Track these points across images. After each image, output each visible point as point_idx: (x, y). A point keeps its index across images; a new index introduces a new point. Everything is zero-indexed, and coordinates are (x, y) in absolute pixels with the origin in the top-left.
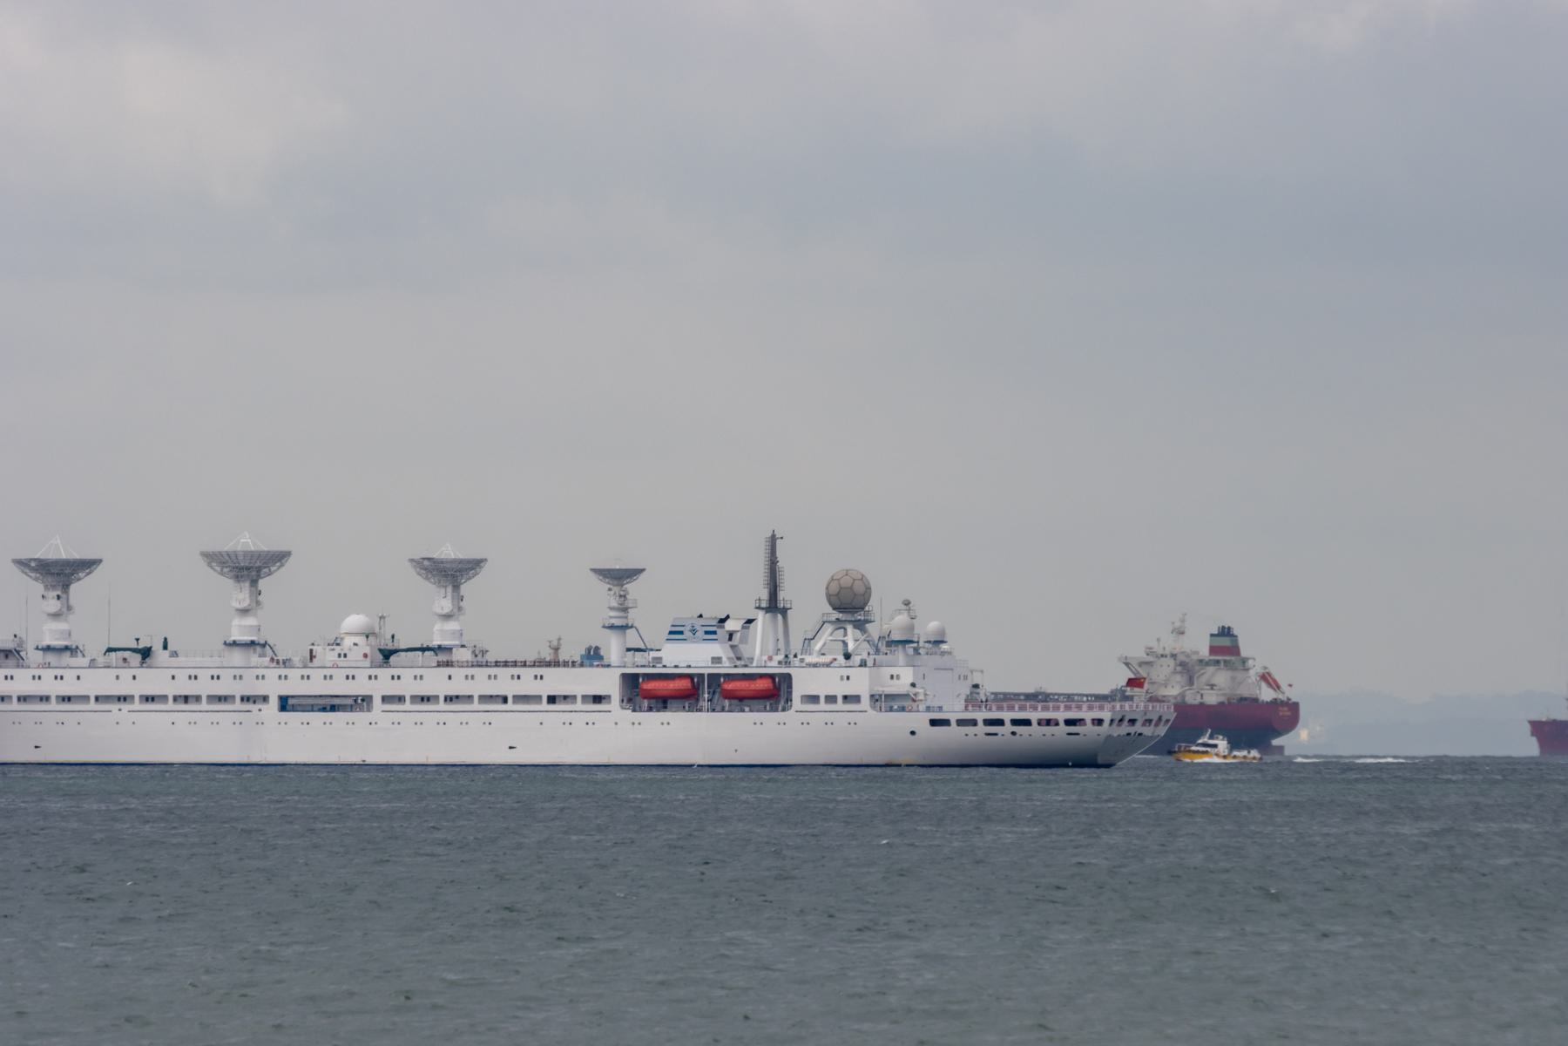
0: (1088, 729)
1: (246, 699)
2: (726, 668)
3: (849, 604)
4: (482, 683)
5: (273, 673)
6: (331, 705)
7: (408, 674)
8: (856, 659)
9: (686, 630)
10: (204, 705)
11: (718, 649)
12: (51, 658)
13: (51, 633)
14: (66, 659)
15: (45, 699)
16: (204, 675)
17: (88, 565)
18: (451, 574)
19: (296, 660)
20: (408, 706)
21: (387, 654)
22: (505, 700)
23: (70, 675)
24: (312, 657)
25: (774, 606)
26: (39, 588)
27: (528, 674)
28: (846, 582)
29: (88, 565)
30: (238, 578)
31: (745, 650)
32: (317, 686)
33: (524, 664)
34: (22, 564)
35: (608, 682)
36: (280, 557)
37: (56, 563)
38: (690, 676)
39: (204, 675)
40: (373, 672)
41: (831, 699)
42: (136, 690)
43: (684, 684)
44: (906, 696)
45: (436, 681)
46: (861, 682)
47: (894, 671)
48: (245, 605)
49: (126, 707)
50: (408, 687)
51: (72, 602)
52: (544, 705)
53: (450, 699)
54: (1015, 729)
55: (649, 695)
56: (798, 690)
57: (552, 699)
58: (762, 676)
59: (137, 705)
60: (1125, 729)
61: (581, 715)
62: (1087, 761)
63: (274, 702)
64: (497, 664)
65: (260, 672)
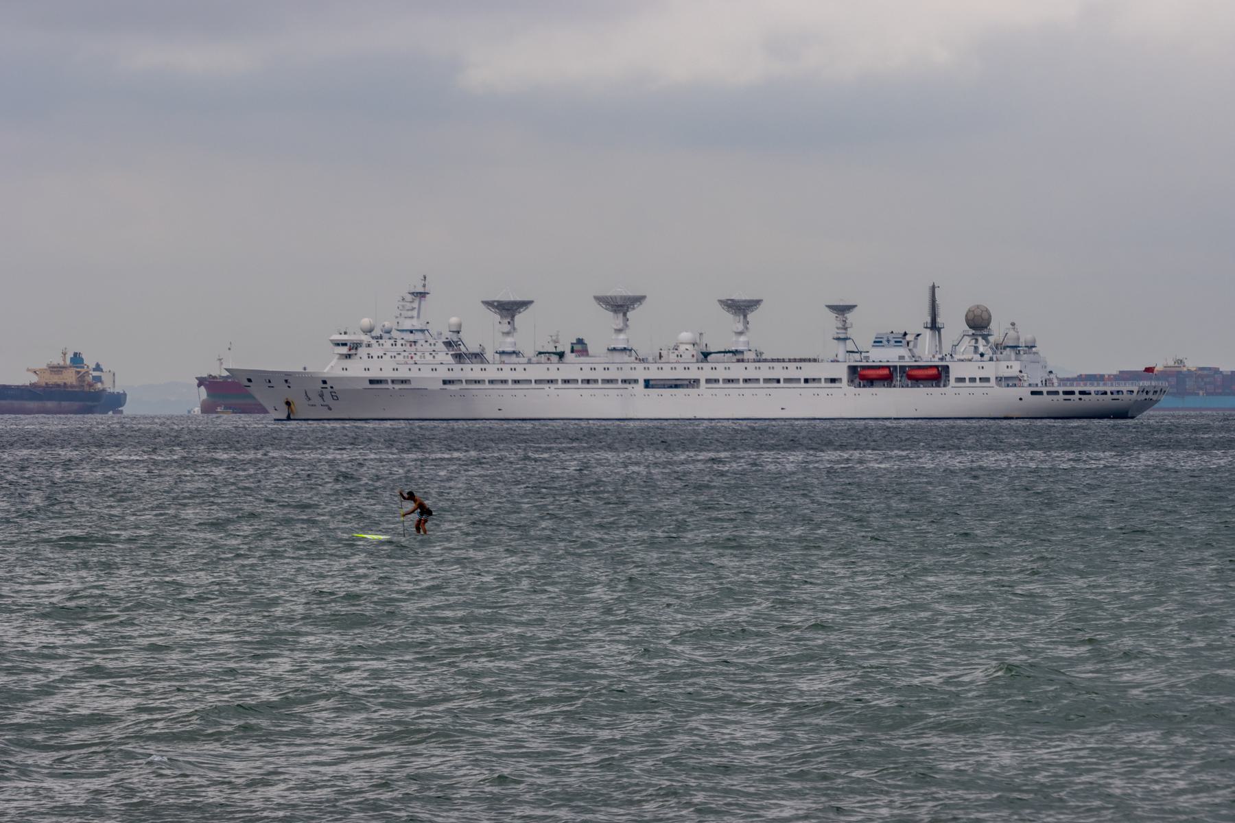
0: (1126, 396)
1: (624, 381)
2: (908, 362)
3: (978, 324)
4: (765, 371)
5: (640, 366)
6: (676, 385)
7: (720, 367)
8: (986, 357)
9: (884, 341)
10: (600, 385)
11: (902, 351)
12: (505, 358)
13: (507, 344)
14: (514, 358)
15: (504, 382)
16: (600, 368)
17: (525, 304)
18: (741, 308)
19: (650, 359)
20: (721, 384)
21: (706, 355)
22: (778, 381)
23: (520, 368)
24: (661, 357)
25: (934, 326)
26: (498, 317)
27: (792, 366)
28: (978, 312)
29: (525, 304)
30: (615, 311)
31: (917, 352)
32: (667, 374)
33: (790, 361)
34: (489, 304)
35: (842, 372)
36: (639, 299)
37: (509, 303)
38: (889, 367)
39: (600, 368)
40: (700, 365)
41: (973, 380)
42: (560, 376)
43: (886, 372)
44: (1016, 378)
45: (738, 371)
46: (990, 370)
47: (1009, 363)
48: (621, 326)
49: (553, 386)
50: (721, 374)
51: (516, 325)
52: (802, 384)
53: (746, 381)
54: (1083, 397)
55: (862, 378)
56: (953, 375)
57: (806, 381)
58: (931, 367)
59: (560, 385)
60: (1144, 396)
61: (824, 390)
62: (1122, 414)
63: (642, 383)
64: (773, 360)
65: (633, 365)
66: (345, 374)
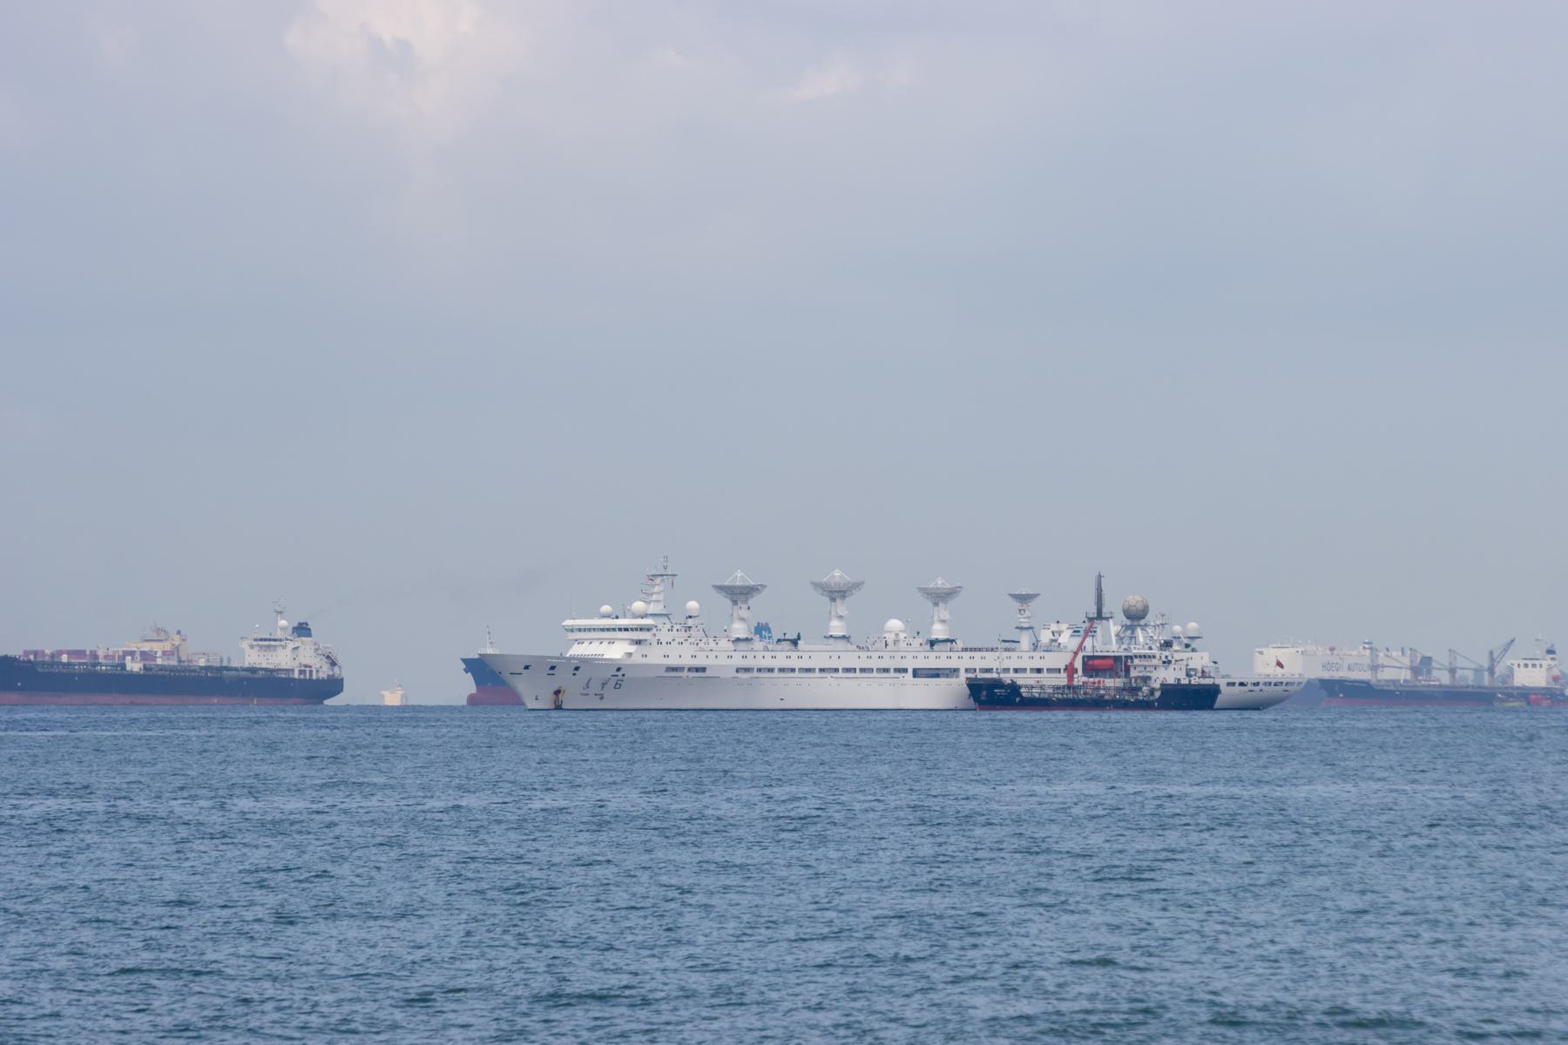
15: (793, 670)
66: (644, 661)
